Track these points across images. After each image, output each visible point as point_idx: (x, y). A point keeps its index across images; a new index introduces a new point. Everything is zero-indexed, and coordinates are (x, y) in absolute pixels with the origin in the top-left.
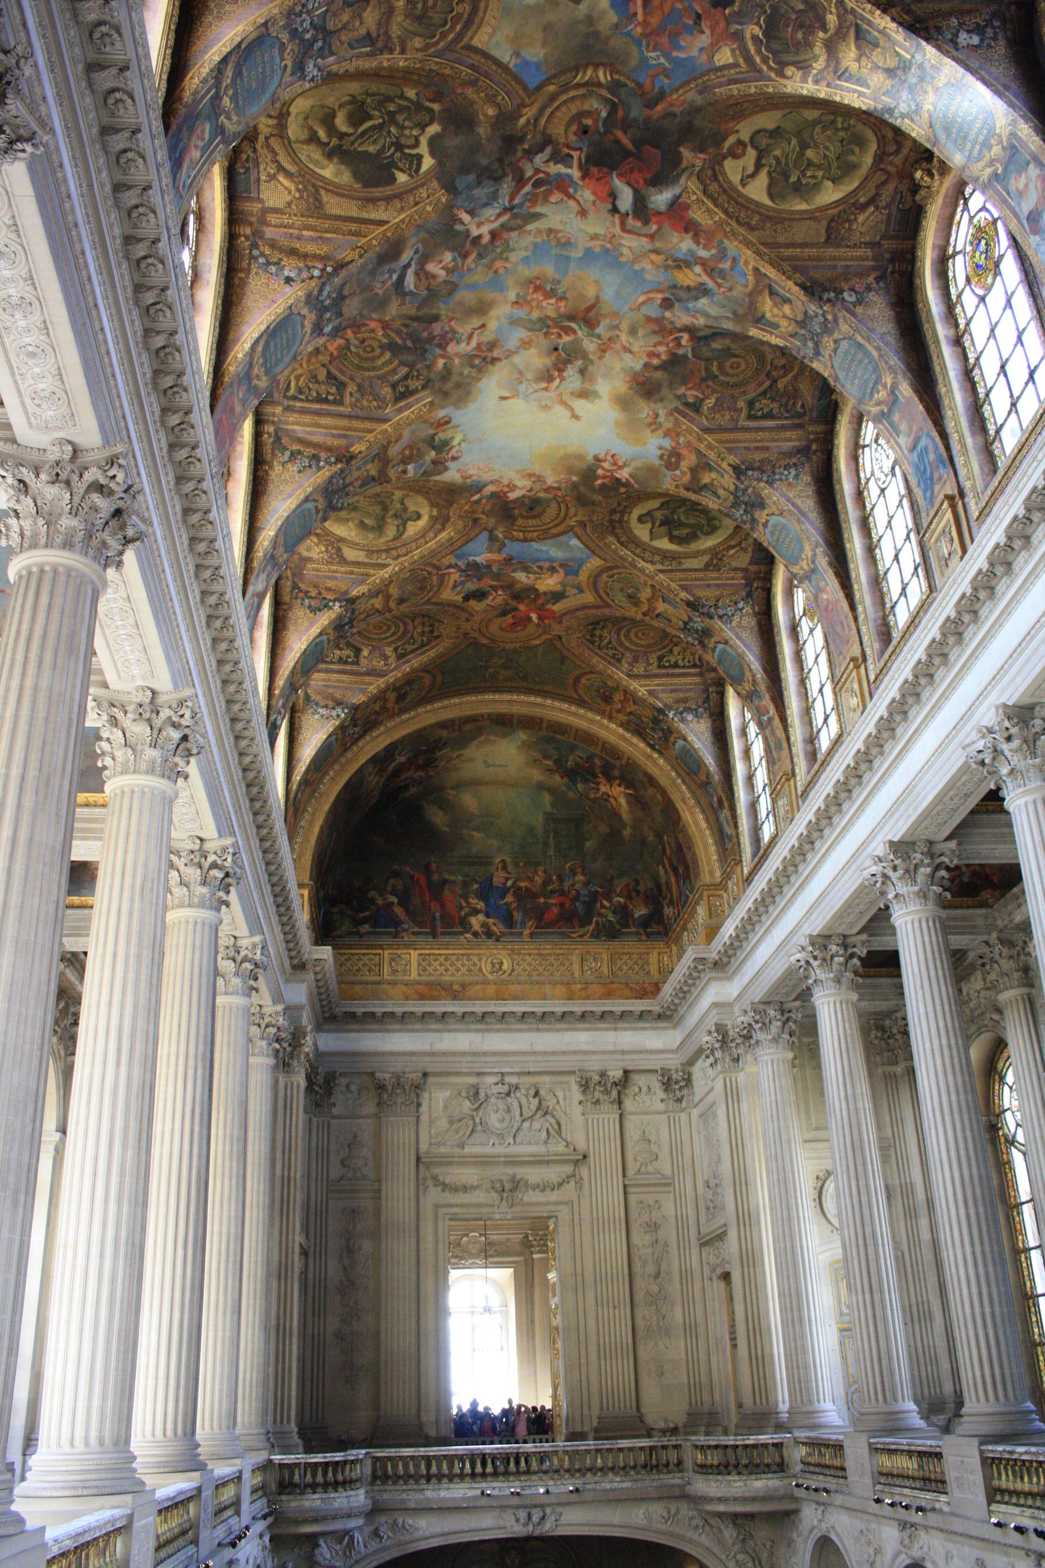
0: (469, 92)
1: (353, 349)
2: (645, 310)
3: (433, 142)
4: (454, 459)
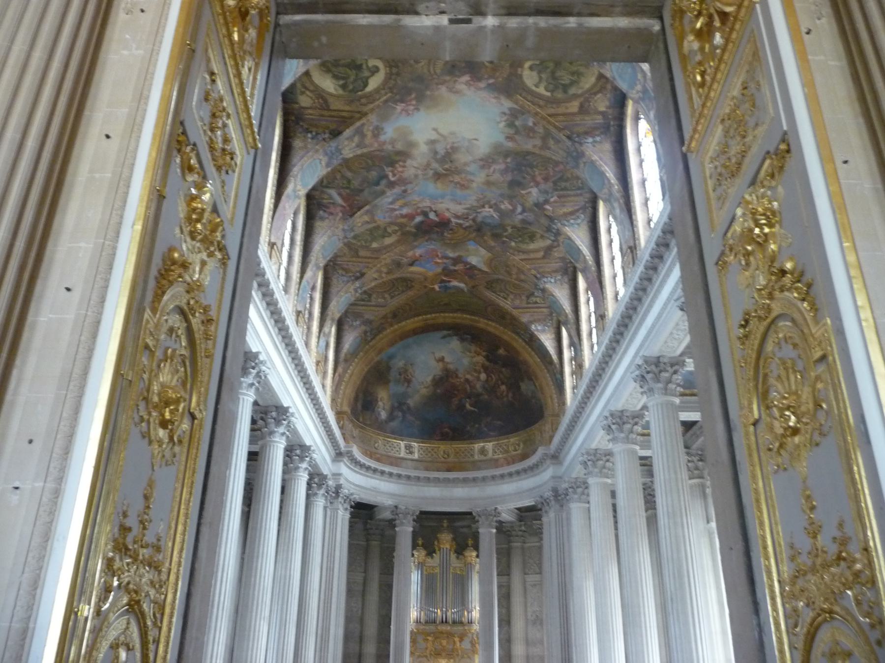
0: (492, 244)
3: (506, 230)
4: (504, 114)
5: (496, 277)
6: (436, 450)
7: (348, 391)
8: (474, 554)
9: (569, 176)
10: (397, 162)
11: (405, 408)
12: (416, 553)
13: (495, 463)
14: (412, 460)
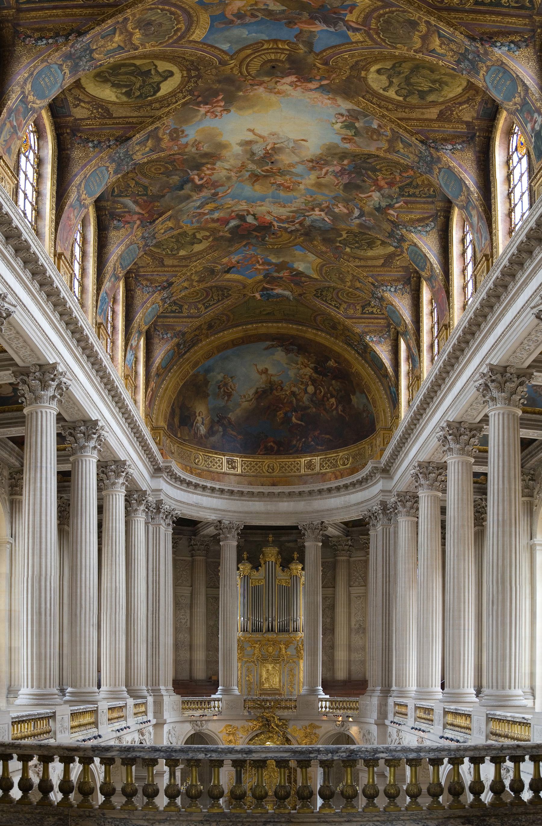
1: (399, 171)
2: (227, 188)
5: (327, 284)
7: (163, 407)
8: (300, 567)
9: (420, 183)
10: (204, 164)
12: (241, 567)
13: (323, 477)
14: (235, 475)
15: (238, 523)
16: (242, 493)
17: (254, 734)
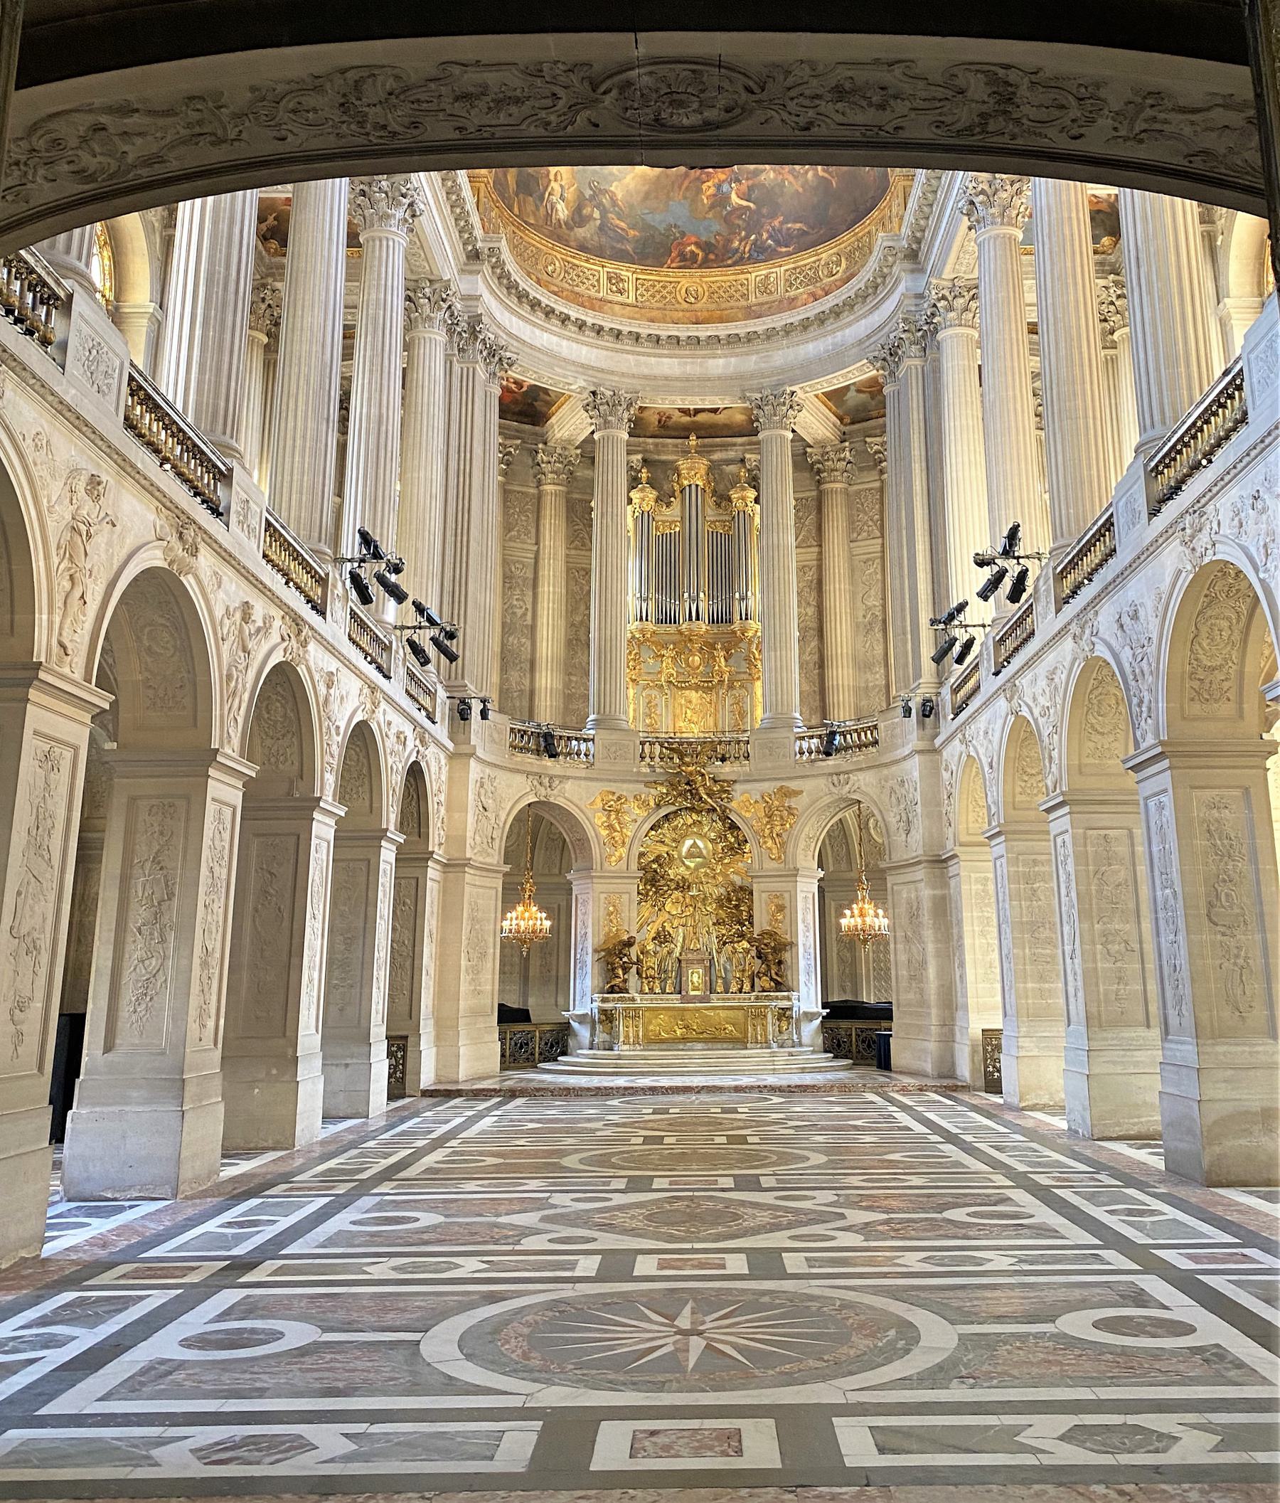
6: (670, 288)
11: (606, 201)
15: (629, 396)
16: (637, 337)
17: (663, 812)
